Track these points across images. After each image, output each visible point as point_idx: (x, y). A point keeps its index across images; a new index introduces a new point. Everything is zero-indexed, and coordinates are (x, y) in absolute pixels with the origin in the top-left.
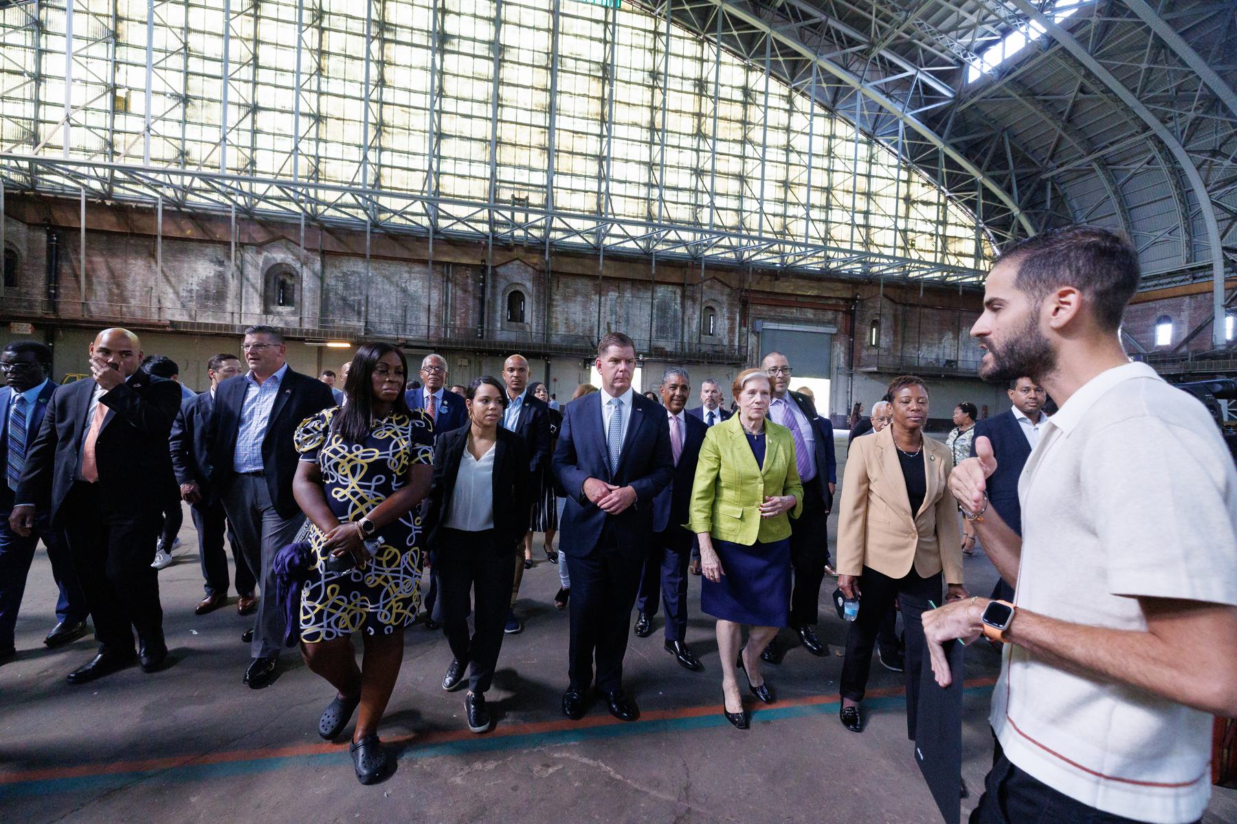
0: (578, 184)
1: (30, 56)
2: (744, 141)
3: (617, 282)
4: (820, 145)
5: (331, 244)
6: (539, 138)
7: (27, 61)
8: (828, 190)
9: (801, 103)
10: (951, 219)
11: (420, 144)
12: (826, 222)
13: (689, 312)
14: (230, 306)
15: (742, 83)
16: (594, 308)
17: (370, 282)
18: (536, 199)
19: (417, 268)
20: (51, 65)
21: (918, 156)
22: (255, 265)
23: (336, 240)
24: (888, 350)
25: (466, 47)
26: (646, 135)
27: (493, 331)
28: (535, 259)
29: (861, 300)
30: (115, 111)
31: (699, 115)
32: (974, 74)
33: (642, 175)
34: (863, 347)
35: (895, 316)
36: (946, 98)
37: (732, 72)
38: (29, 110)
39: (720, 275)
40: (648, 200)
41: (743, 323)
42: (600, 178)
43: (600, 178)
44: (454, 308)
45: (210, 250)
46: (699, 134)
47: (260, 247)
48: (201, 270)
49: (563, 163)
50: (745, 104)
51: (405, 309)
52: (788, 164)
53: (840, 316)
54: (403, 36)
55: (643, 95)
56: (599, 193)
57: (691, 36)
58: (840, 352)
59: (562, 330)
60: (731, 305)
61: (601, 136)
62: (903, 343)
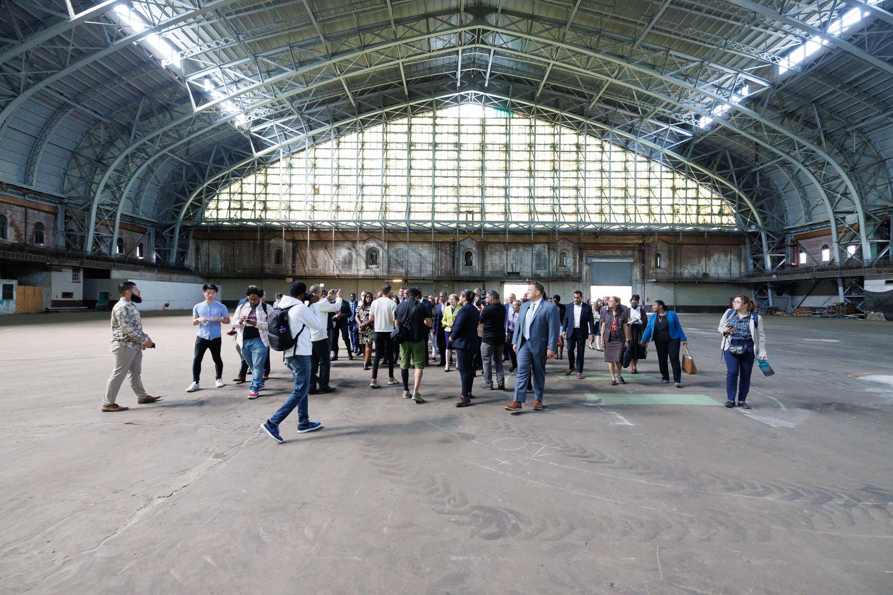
0: (495, 200)
1: (288, 177)
2: (578, 170)
3: (515, 244)
4: (619, 166)
6: (477, 182)
7: (287, 180)
8: (625, 189)
9: (607, 146)
10: (700, 196)
12: (625, 205)
13: (552, 257)
14: (354, 266)
15: (576, 142)
16: (504, 257)
17: (407, 252)
18: (477, 210)
20: (294, 180)
21: (677, 167)
22: (362, 249)
23: (393, 235)
24: (666, 269)
25: (444, 147)
26: (527, 174)
27: (458, 271)
28: (477, 236)
30: (315, 194)
31: (554, 161)
32: (784, 67)
33: (526, 193)
34: (650, 268)
35: (669, 251)
36: (688, 137)
37: (569, 137)
38: (287, 198)
41: (581, 260)
44: (441, 261)
45: (346, 244)
46: (554, 170)
47: (364, 241)
49: (488, 192)
50: (577, 152)
52: (602, 178)
53: (636, 253)
54: (419, 147)
55: (526, 155)
57: (548, 124)
58: (637, 272)
59: (490, 269)
61: (505, 177)
62: (675, 265)
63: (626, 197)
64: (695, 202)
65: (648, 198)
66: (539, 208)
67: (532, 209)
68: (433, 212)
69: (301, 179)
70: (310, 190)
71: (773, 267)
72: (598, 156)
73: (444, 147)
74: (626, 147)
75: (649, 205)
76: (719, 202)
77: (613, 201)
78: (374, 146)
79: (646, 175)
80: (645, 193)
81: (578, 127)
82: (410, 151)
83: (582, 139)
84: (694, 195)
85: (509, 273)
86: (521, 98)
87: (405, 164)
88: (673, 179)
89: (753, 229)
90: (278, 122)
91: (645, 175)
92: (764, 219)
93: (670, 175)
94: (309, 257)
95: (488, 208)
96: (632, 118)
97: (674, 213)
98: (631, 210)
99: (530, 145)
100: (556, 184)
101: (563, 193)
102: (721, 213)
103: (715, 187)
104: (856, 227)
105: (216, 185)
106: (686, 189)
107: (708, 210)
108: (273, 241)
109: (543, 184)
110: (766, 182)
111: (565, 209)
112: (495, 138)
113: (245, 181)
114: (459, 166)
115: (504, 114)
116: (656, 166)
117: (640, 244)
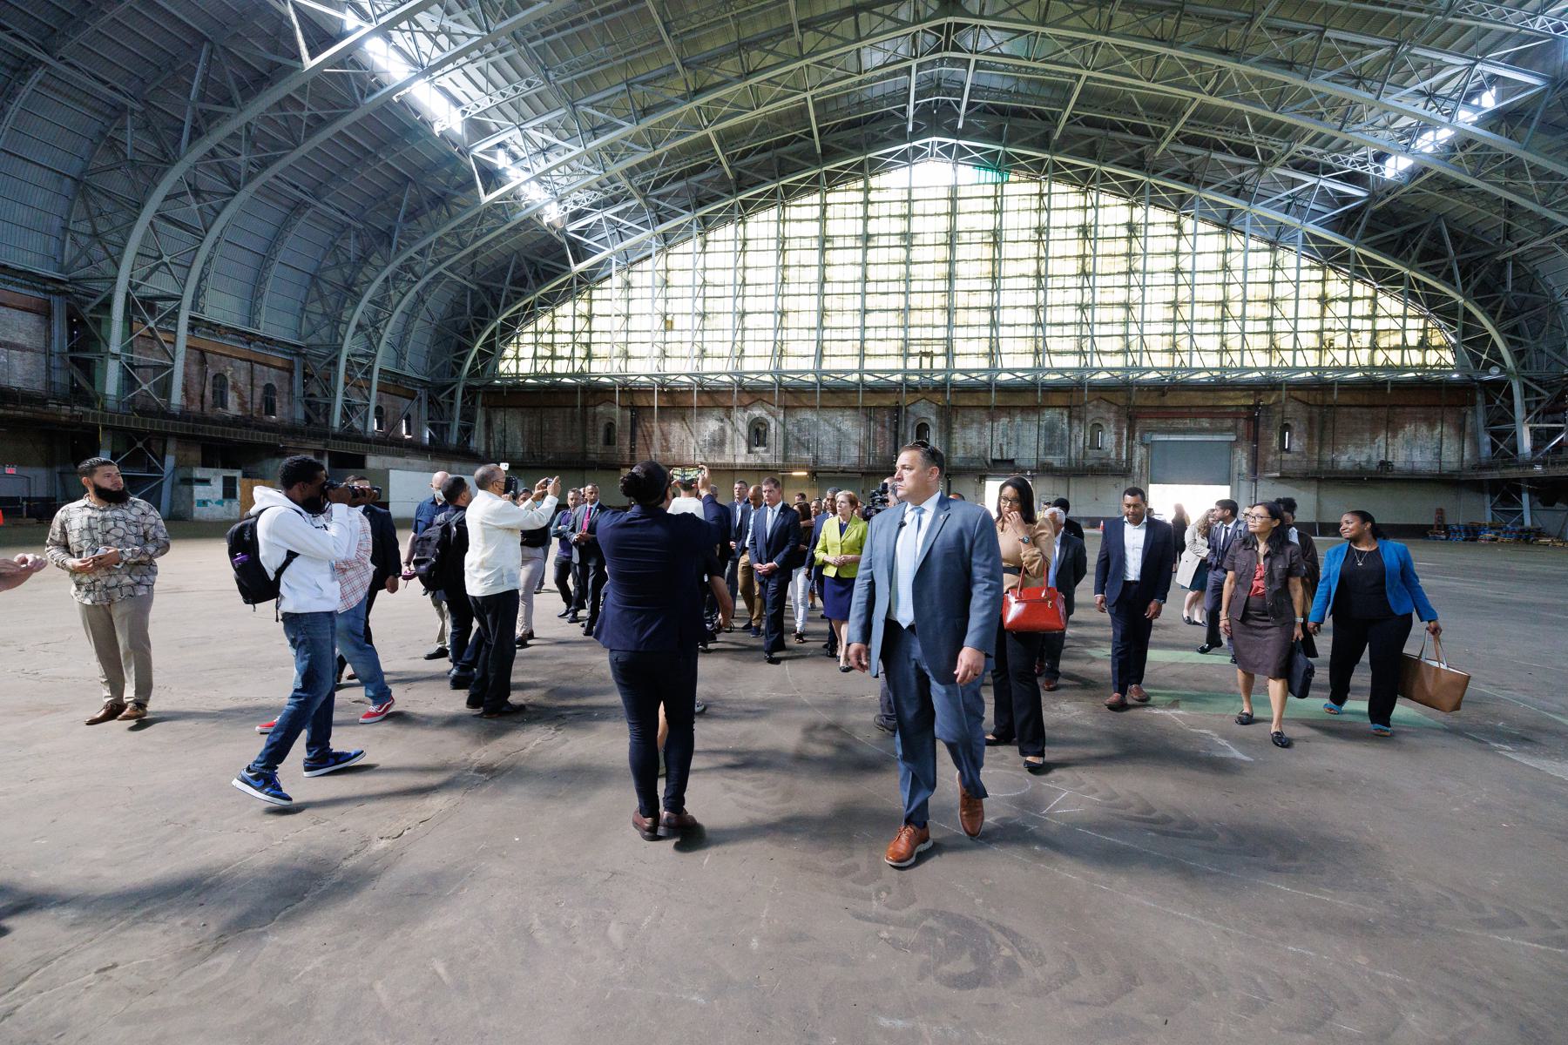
0: (973, 332)
1: (624, 303)
2: (1130, 272)
3: (1007, 410)
4: (1213, 262)
5: (791, 402)
6: (940, 300)
7: (621, 307)
8: (1224, 304)
9: (1188, 225)
11: (854, 320)
12: (1222, 334)
14: (728, 449)
15: (1126, 219)
16: (987, 432)
17: (816, 425)
18: (938, 349)
19: (848, 412)
20: (635, 307)
21: (1331, 258)
22: (742, 420)
23: (793, 396)
25: (883, 241)
26: (1033, 283)
28: (939, 396)
29: (1267, 407)
30: (666, 330)
31: (1083, 257)
33: (1030, 317)
34: (1268, 451)
35: (1310, 420)
37: (1114, 211)
38: (622, 337)
39: (1104, 395)
40: (1036, 337)
41: (1131, 437)
45: (716, 412)
46: (1084, 274)
47: (746, 407)
48: (711, 426)
49: (961, 317)
50: (1129, 239)
51: (840, 444)
53: (1242, 424)
54: (838, 243)
55: (1032, 249)
56: (991, 338)
57: (1074, 189)
58: (1242, 460)
59: (960, 453)
60: (1118, 421)
61: (992, 291)
63: (1223, 319)
64: (1368, 324)
65: (1270, 320)
66: (1053, 345)
67: (1041, 345)
69: (645, 305)
70: (658, 323)
71: (1535, 449)
72: (1171, 244)
73: (883, 241)
74: (1227, 223)
75: (1271, 333)
76: (1420, 323)
77: (1197, 328)
78: (762, 245)
80: (1265, 311)
81: (1133, 192)
82: (823, 250)
83: (1138, 214)
84: (1368, 311)
85: (994, 461)
86: (1025, 145)
87: (813, 274)
88: (1324, 281)
89: (1495, 373)
90: (609, 213)
91: (1265, 275)
92: (1519, 355)
93: (1318, 275)
94: (657, 432)
95: (959, 346)
96: (1241, 168)
97: (1324, 347)
98: (1234, 342)
100: (1087, 299)
102: (1423, 345)
105: (514, 321)
106: (1350, 299)
108: (601, 409)
109: (1063, 301)
110: (1528, 281)
111: (1102, 344)
112: (976, 219)
113: (558, 311)
114: (908, 274)
115: (991, 176)
116: (1289, 259)
117: (1249, 407)
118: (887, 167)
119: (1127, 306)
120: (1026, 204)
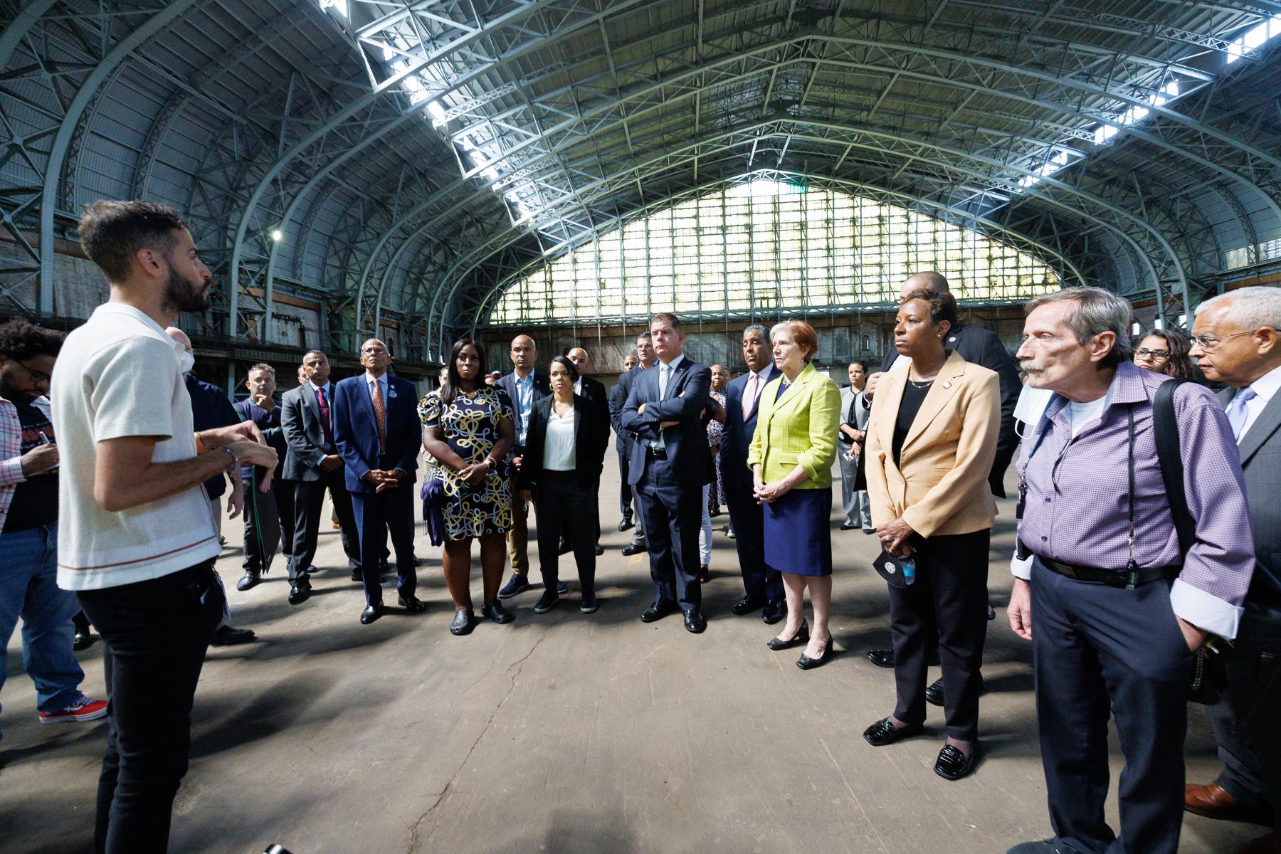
2: (881, 245)
6: (771, 265)
9: (913, 216)
21: (992, 235)
26: (825, 253)
31: (854, 237)
37: (870, 209)
42: (802, 279)
43: (802, 279)
46: (855, 247)
50: (880, 225)
64: (1014, 272)
65: (961, 271)
68: (726, 300)
69: (587, 271)
70: (595, 285)
73: (734, 230)
74: (934, 216)
75: (962, 279)
78: (659, 234)
79: (958, 245)
80: (958, 266)
81: (882, 199)
82: (698, 236)
83: (885, 211)
84: (1014, 264)
86: (817, 173)
87: (694, 250)
90: (564, 219)
91: (958, 245)
93: (987, 244)
94: (599, 354)
95: (784, 293)
96: (941, 185)
97: (991, 286)
99: (827, 221)
100: (858, 262)
101: (866, 271)
102: (1045, 283)
103: (1036, 253)
104: (1180, 296)
105: (503, 287)
106: (1003, 258)
107: (1029, 281)
109: (843, 260)
110: (1096, 247)
111: (867, 289)
112: (789, 216)
113: (530, 279)
115: (797, 189)
116: (969, 234)
118: (735, 185)
119: (880, 265)
120: (819, 206)
